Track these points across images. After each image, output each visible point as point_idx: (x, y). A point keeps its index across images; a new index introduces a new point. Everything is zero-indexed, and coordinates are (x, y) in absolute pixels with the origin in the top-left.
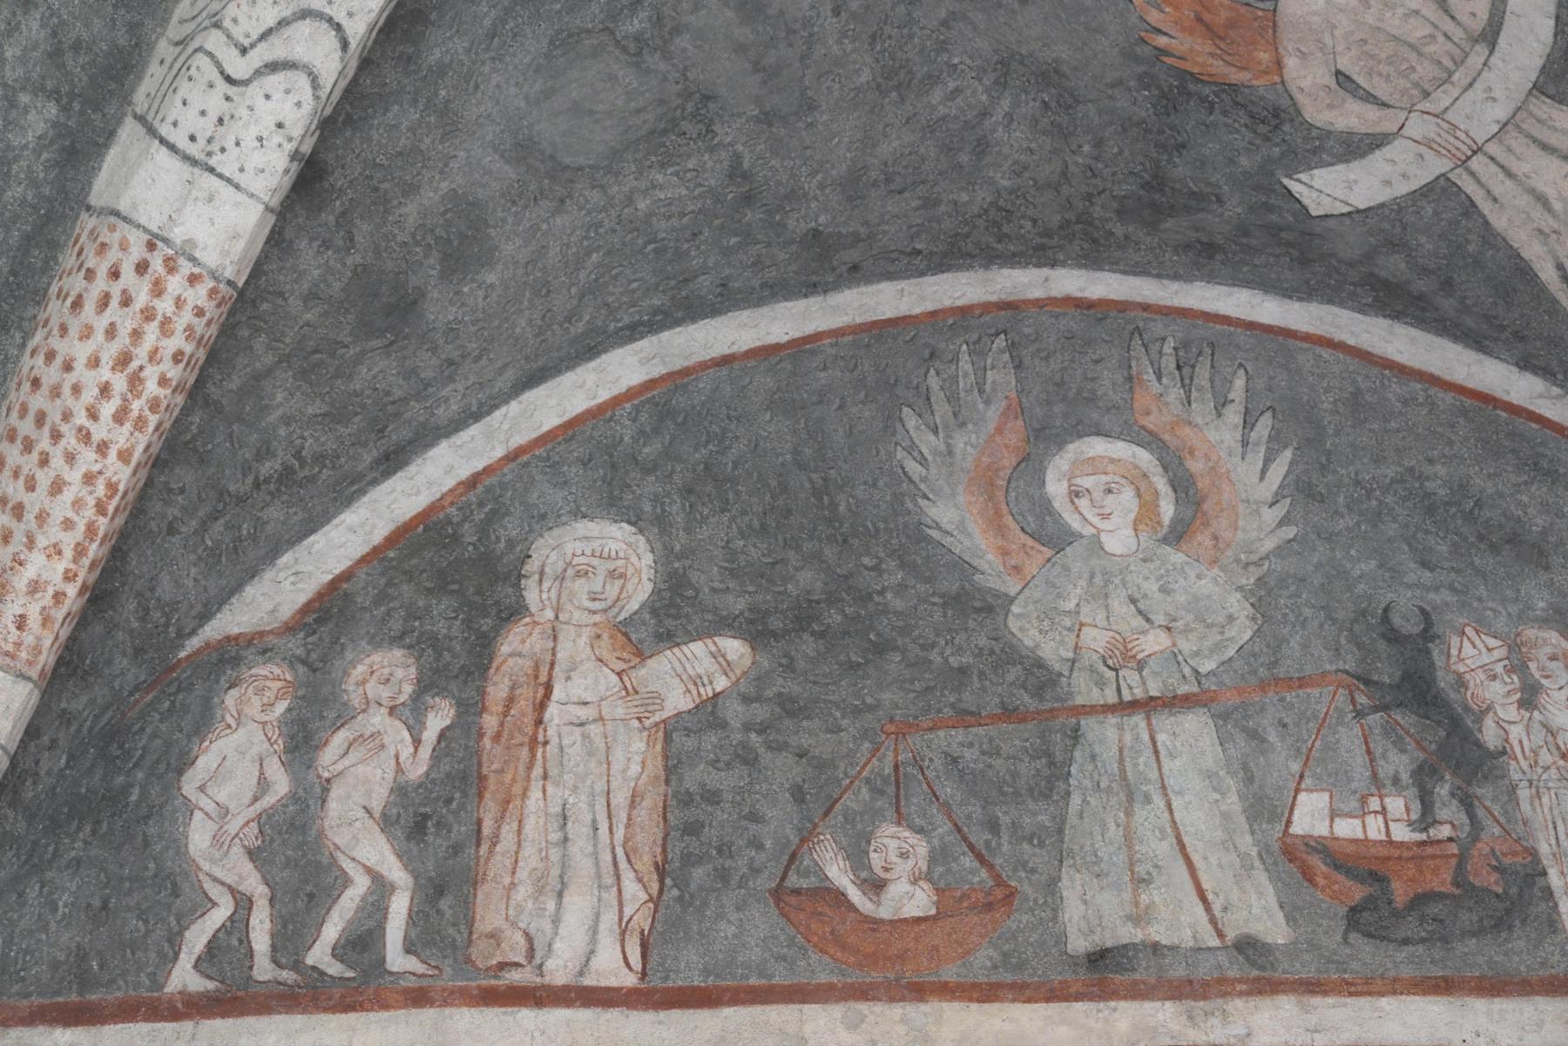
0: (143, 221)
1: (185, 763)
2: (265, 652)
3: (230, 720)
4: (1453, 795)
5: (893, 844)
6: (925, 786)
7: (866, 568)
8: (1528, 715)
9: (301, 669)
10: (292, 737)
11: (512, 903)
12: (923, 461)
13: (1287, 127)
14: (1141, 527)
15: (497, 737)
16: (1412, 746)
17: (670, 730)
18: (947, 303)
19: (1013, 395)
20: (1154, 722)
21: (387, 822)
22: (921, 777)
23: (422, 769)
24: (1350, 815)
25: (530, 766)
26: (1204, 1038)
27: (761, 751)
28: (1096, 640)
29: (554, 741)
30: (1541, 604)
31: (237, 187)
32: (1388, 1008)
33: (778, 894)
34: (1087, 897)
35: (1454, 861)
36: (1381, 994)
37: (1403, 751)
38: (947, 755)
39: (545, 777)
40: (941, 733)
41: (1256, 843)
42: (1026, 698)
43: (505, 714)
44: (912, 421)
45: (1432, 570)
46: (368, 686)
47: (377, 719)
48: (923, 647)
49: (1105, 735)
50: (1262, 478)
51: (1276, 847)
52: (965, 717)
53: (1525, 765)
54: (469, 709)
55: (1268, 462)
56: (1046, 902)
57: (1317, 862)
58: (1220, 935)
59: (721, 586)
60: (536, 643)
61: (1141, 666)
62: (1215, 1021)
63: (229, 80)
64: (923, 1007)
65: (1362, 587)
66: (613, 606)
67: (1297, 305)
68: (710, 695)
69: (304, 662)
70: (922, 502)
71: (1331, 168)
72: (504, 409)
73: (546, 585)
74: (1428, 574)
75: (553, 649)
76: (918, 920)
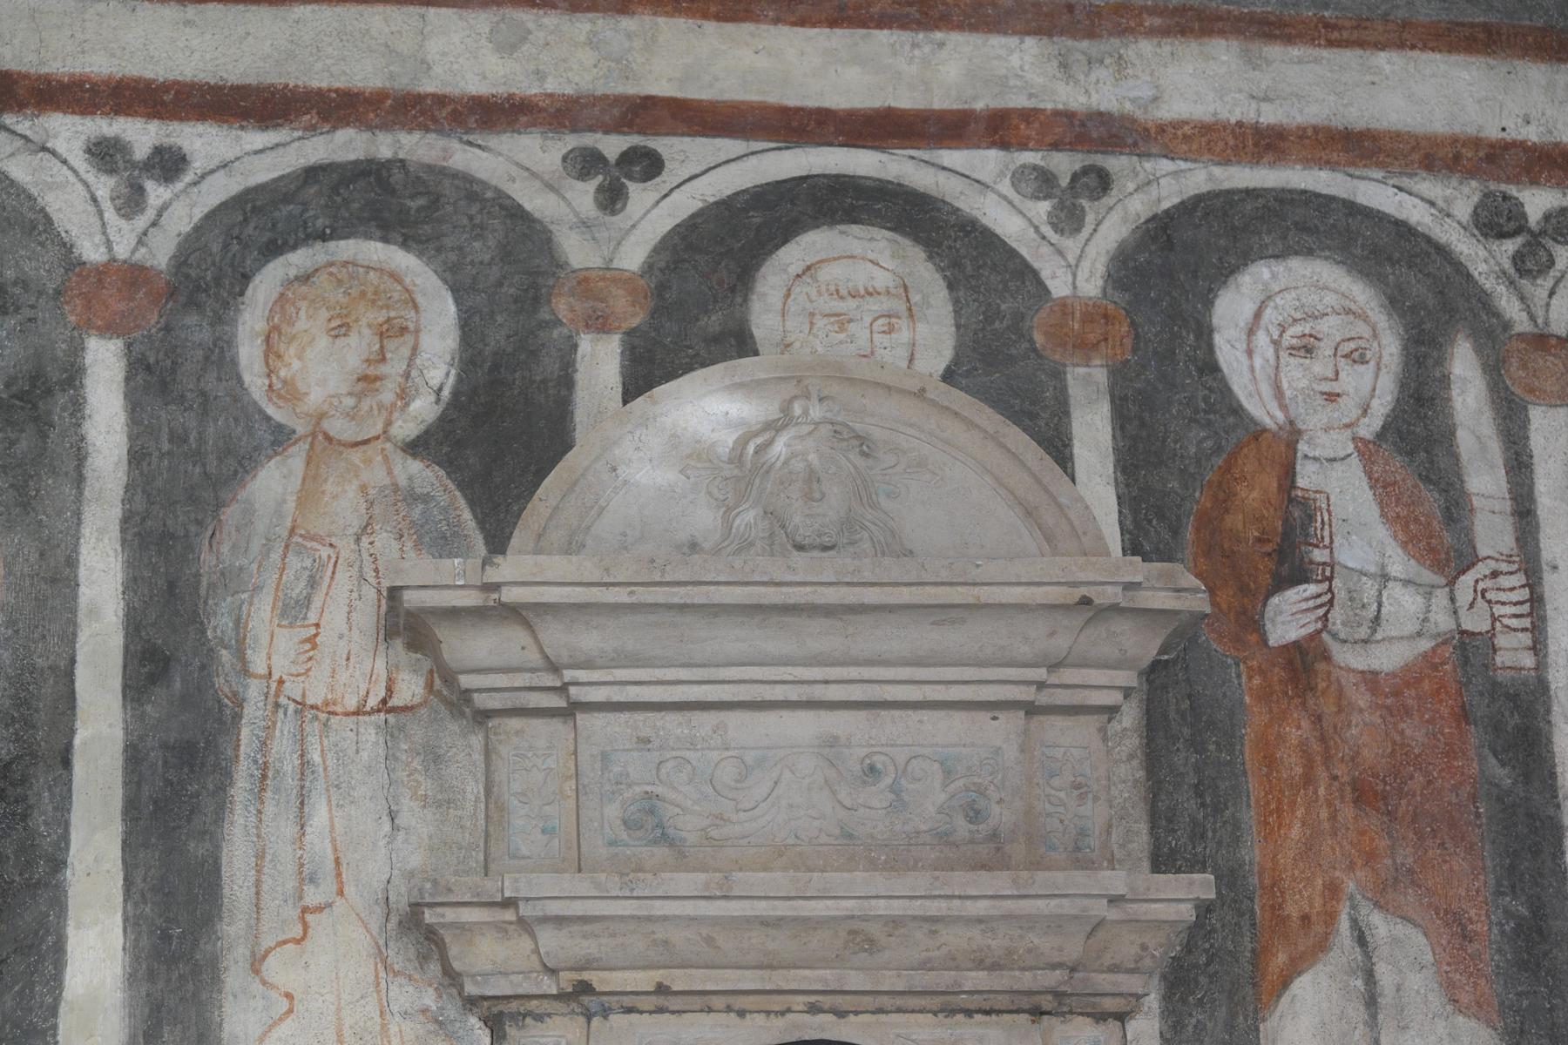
26: (1083, 99)
32: (1387, 68)
36: (1380, 46)
62: (1100, 73)
64: (627, 23)
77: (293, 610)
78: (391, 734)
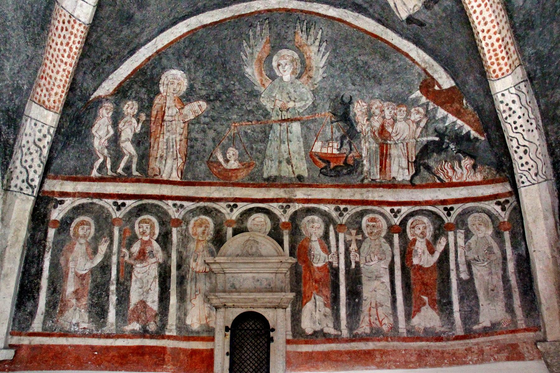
12: (246, 56)
17: (190, 123)
33: (208, 162)
43: (156, 118)
45: (354, 85)
77: (195, 261)
78: (205, 275)
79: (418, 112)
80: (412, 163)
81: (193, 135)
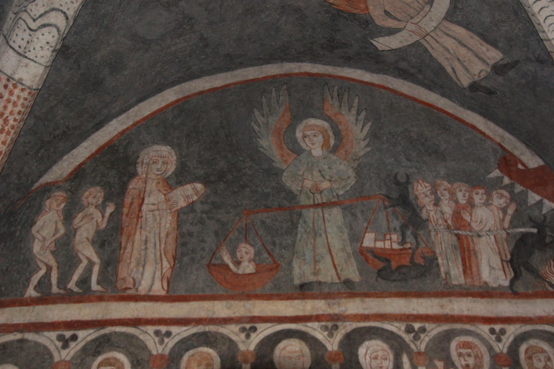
0: (5, 72)
1: (33, 223)
2: (58, 187)
3: (47, 209)
4: (412, 234)
5: (244, 250)
6: (254, 231)
7: (241, 161)
8: (436, 208)
9: (69, 193)
10: (66, 215)
11: (130, 268)
12: (259, 126)
13: (370, 26)
14: (324, 147)
15: (127, 215)
16: (400, 218)
18: (269, 74)
19: (288, 104)
20: (324, 210)
21: (93, 243)
22: (253, 228)
23: (104, 225)
24: (380, 240)
25: (137, 225)
27: (206, 220)
28: (308, 184)
29: (144, 216)
30: (443, 173)
31: (35, 62)
33: (209, 266)
34: (301, 267)
35: (410, 255)
37: (398, 220)
38: (261, 221)
39: (141, 228)
40: (260, 214)
41: (352, 249)
42: (286, 203)
44: (257, 113)
45: (410, 162)
46: (89, 199)
47: (92, 209)
48: (256, 186)
49: (309, 214)
50: (361, 131)
51: (358, 250)
52: (267, 209)
53: (434, 224)
54: (119, 207)
55: (363, 126)
56: (288, 269)
57: (369, 255)
58: (339, 278)
59: (197, 166)
60: (140, 185)
61: (321, 192)
63: (30, 29)
65: (389, 167)
66: (164, 173)
67: (375, 75)
68: (192, 201)
69: (70, 191)
70: (258, 139)
71: (384, 37)
72: (133, 109)
73: (144, 166)
74: (409, 163)
75: (145, 187)
76: (250, 274)
79: (502, 196)
80: (507, 262)
81: (186, 228)
